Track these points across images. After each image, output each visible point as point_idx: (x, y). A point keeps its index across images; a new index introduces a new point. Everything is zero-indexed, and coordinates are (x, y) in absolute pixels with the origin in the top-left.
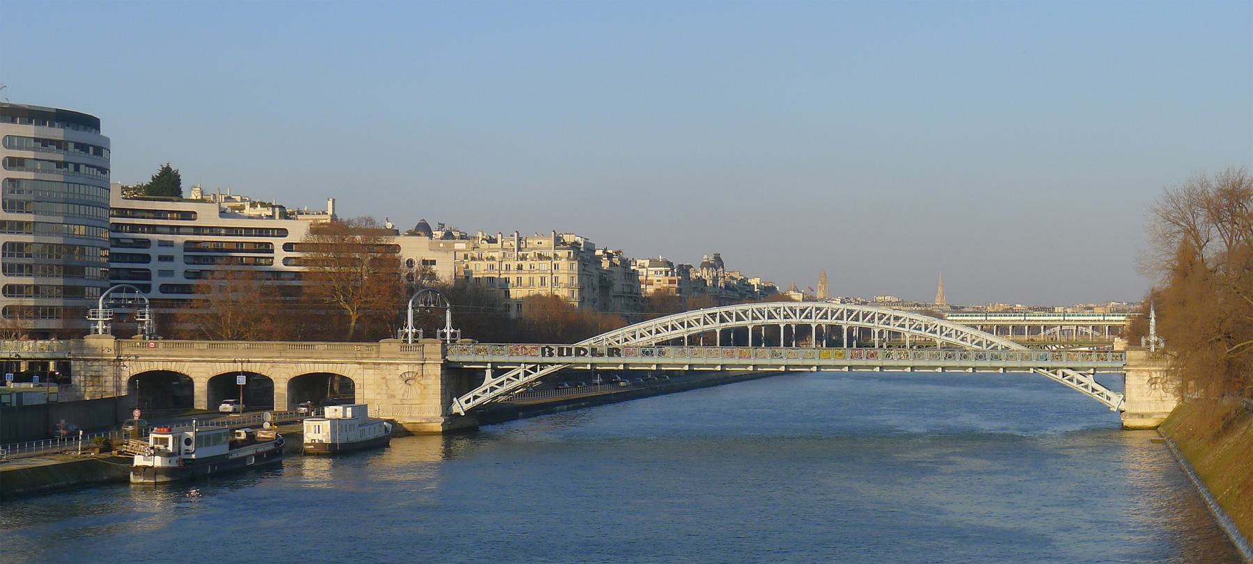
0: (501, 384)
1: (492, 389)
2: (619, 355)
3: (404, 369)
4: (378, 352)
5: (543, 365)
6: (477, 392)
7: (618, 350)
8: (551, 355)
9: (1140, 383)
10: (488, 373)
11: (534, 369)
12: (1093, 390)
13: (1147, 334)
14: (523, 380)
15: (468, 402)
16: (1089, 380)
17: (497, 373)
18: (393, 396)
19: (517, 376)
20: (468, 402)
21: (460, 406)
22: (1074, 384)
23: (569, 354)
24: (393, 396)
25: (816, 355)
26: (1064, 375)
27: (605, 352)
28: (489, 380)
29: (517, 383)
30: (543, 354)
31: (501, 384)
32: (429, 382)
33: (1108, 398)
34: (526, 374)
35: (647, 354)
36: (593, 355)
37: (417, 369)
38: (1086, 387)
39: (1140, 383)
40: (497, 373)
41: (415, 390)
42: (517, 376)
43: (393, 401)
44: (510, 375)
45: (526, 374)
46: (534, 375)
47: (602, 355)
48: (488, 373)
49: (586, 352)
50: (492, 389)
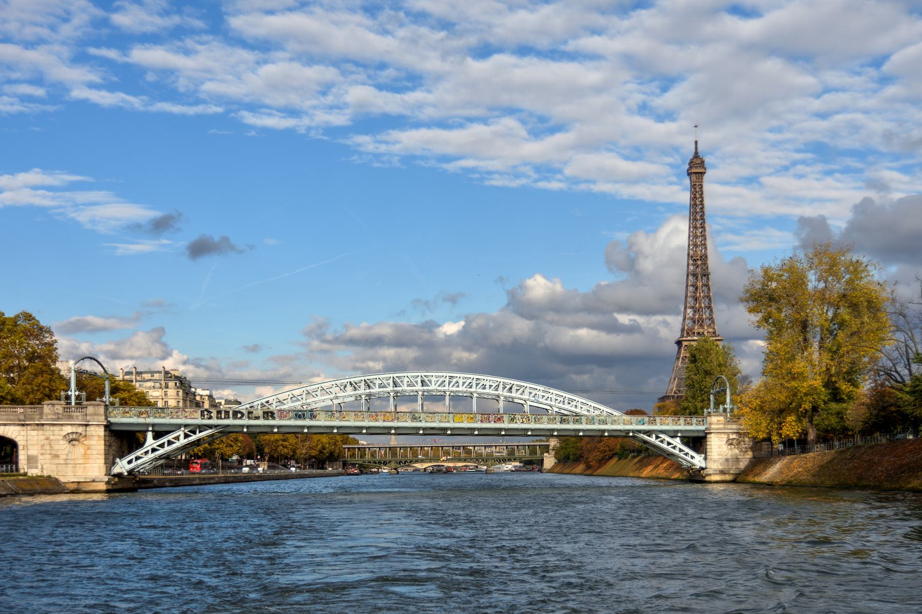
0: (162, 446)
1: (154, 450)
2: (274, 418)
3: (69, 429)
4: (41, 414)
5: (202, 428)
6: (139, 453)
7: (272, 413)
8: (210, 418)
9: (720, 443)
10: (150, 435)
11: (194, 433)
12: (681, 450)
13: (724, 403)
14: (183, 441)
15: (130, 462)
16: (677, 442)
17: (158, 435)
18: (57, 456)
19: (177, 438)
20: (130, 462)
21: (122, 466)
22: (664, 446)
23: (227, 417)
24: (57, 456)
25: (451, 419)
26: (657, 437)
27: (260, 413)
28: (150, 441)
29: (177, 444)
30: (202, 415)
31: (162, 446)
32: (93, 442)
33: (692, 457)
34: (186, 436)
35: (300, 417)
36: (249, 418)
37: (80, 430)
38: (674, 448)
39: (720, 443)
40: (158, 435)
41: (79, 450)
42: (177, 438)
43: (57, 461)
44: (170, 437)
45: (186, 436)
46: (193, 438)
47: (257, 418)
48: (150, 435)
49: (243, 415)
50: (154, 450)
